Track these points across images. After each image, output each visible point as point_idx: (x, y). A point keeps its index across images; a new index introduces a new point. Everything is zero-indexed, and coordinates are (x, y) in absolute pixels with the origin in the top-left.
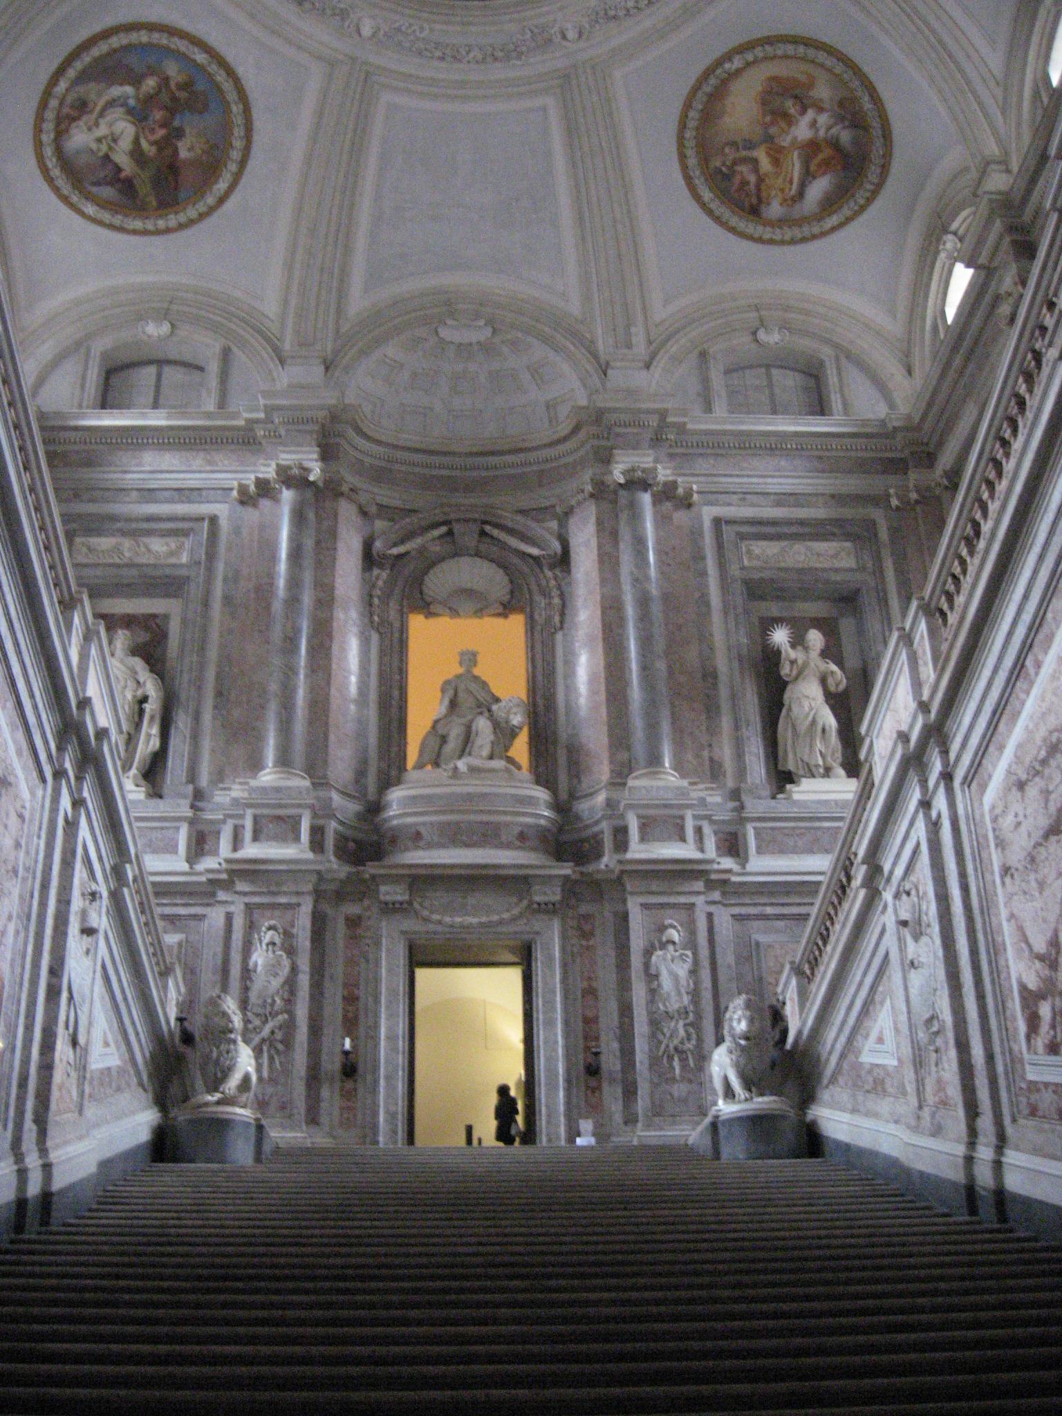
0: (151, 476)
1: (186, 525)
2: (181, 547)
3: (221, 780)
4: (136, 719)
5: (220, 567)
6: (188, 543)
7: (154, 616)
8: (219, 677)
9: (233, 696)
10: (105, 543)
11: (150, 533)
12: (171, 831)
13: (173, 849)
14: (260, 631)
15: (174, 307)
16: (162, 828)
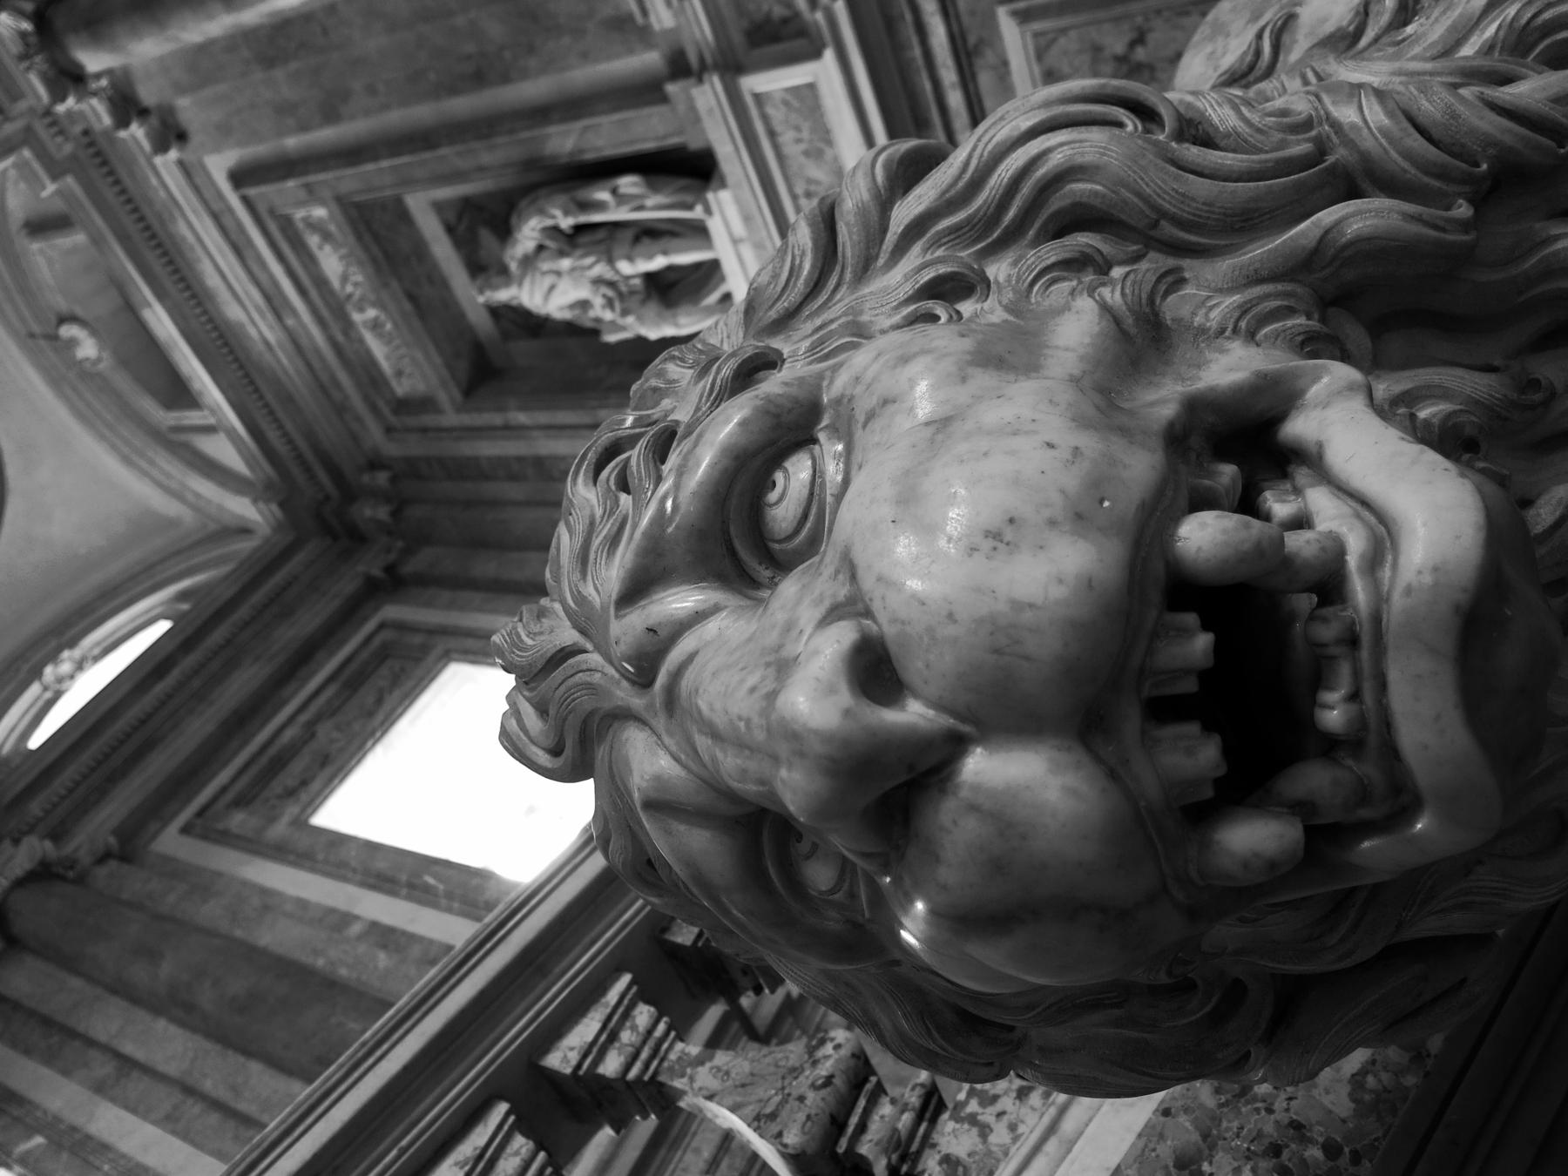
0: (247, 303)
1: (273, 227)
2: (306, 220)
3: (630, 18)
4: (601, 234)
5: (293, 143)
6: (299, 214)
7: (450, 230)
8: (453, 91)
9: (470, 48)
10: (378, 349)
11: (321, 282)
12: (770, 110)
13: (808, 95)
14: (325, 32)
15: (36, 329)
16: (772, 134)
